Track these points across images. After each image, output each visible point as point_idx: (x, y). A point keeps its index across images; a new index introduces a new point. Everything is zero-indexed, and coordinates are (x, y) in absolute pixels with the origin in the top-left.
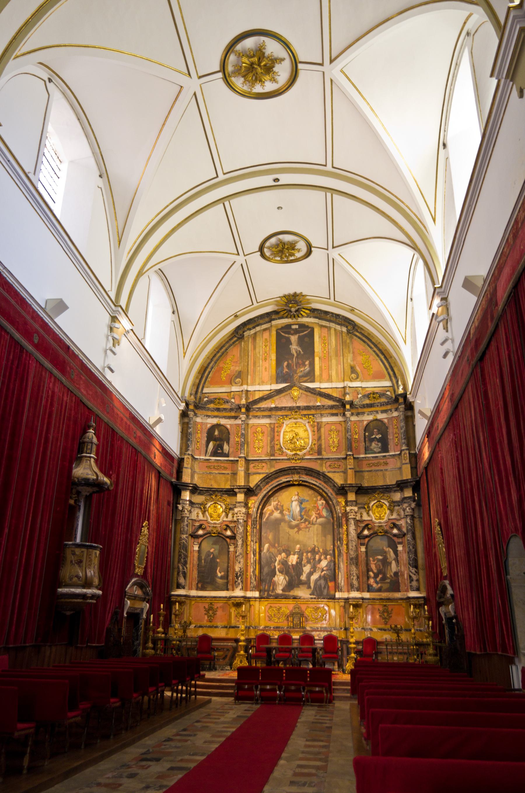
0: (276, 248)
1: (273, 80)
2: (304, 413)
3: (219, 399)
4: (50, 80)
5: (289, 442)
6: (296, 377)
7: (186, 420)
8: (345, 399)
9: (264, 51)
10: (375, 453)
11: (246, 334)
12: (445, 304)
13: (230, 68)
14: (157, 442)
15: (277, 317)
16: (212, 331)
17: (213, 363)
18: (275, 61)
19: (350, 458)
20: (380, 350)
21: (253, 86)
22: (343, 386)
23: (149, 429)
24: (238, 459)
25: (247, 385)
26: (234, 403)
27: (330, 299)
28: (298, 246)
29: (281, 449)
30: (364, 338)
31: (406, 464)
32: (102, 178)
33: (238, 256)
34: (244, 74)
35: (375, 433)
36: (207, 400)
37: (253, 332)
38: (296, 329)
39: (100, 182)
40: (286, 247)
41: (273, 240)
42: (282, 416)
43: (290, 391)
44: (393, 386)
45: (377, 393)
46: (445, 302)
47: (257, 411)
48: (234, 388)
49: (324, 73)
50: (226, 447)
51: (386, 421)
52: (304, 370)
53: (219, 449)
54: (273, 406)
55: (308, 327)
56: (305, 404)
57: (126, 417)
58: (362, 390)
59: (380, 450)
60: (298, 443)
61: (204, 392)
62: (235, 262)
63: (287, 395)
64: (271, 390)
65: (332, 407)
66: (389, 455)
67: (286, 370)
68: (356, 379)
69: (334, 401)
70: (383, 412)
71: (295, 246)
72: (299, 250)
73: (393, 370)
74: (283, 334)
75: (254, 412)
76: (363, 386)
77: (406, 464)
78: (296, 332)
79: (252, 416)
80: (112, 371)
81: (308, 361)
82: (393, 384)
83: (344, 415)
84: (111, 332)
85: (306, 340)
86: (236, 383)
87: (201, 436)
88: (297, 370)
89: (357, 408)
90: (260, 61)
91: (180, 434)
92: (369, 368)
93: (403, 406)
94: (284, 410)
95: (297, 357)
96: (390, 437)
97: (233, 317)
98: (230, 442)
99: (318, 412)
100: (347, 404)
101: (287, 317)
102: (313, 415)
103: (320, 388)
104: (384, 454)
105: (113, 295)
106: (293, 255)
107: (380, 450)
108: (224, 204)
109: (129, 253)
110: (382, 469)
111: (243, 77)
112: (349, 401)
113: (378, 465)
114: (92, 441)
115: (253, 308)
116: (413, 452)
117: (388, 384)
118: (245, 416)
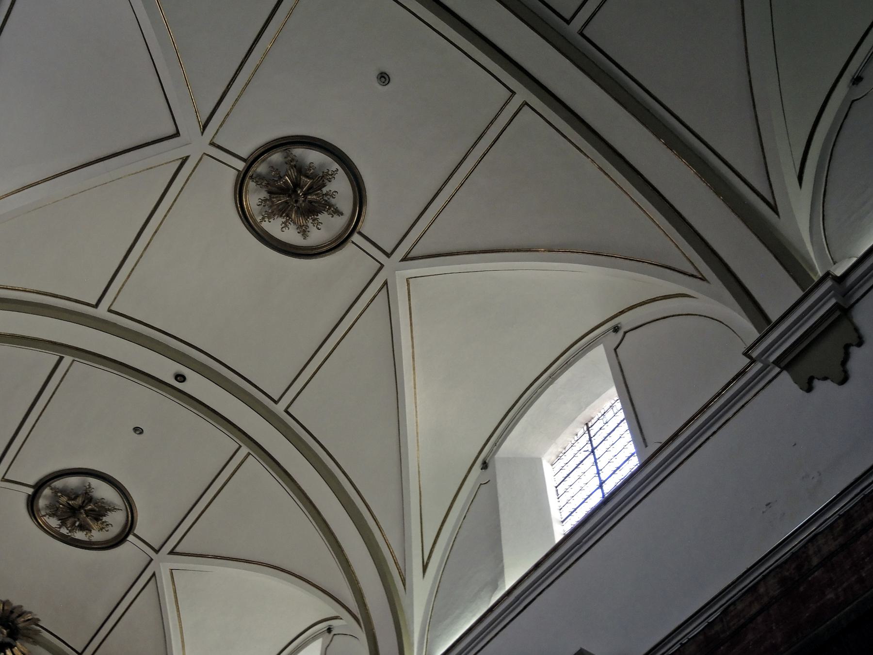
1: (304, 231)
13: (261, 168)
21: (270, 216)
28: (110, 518)
34: (274, 189)
41: (73, 482)
108: (61, 358)
111: (269, 192)
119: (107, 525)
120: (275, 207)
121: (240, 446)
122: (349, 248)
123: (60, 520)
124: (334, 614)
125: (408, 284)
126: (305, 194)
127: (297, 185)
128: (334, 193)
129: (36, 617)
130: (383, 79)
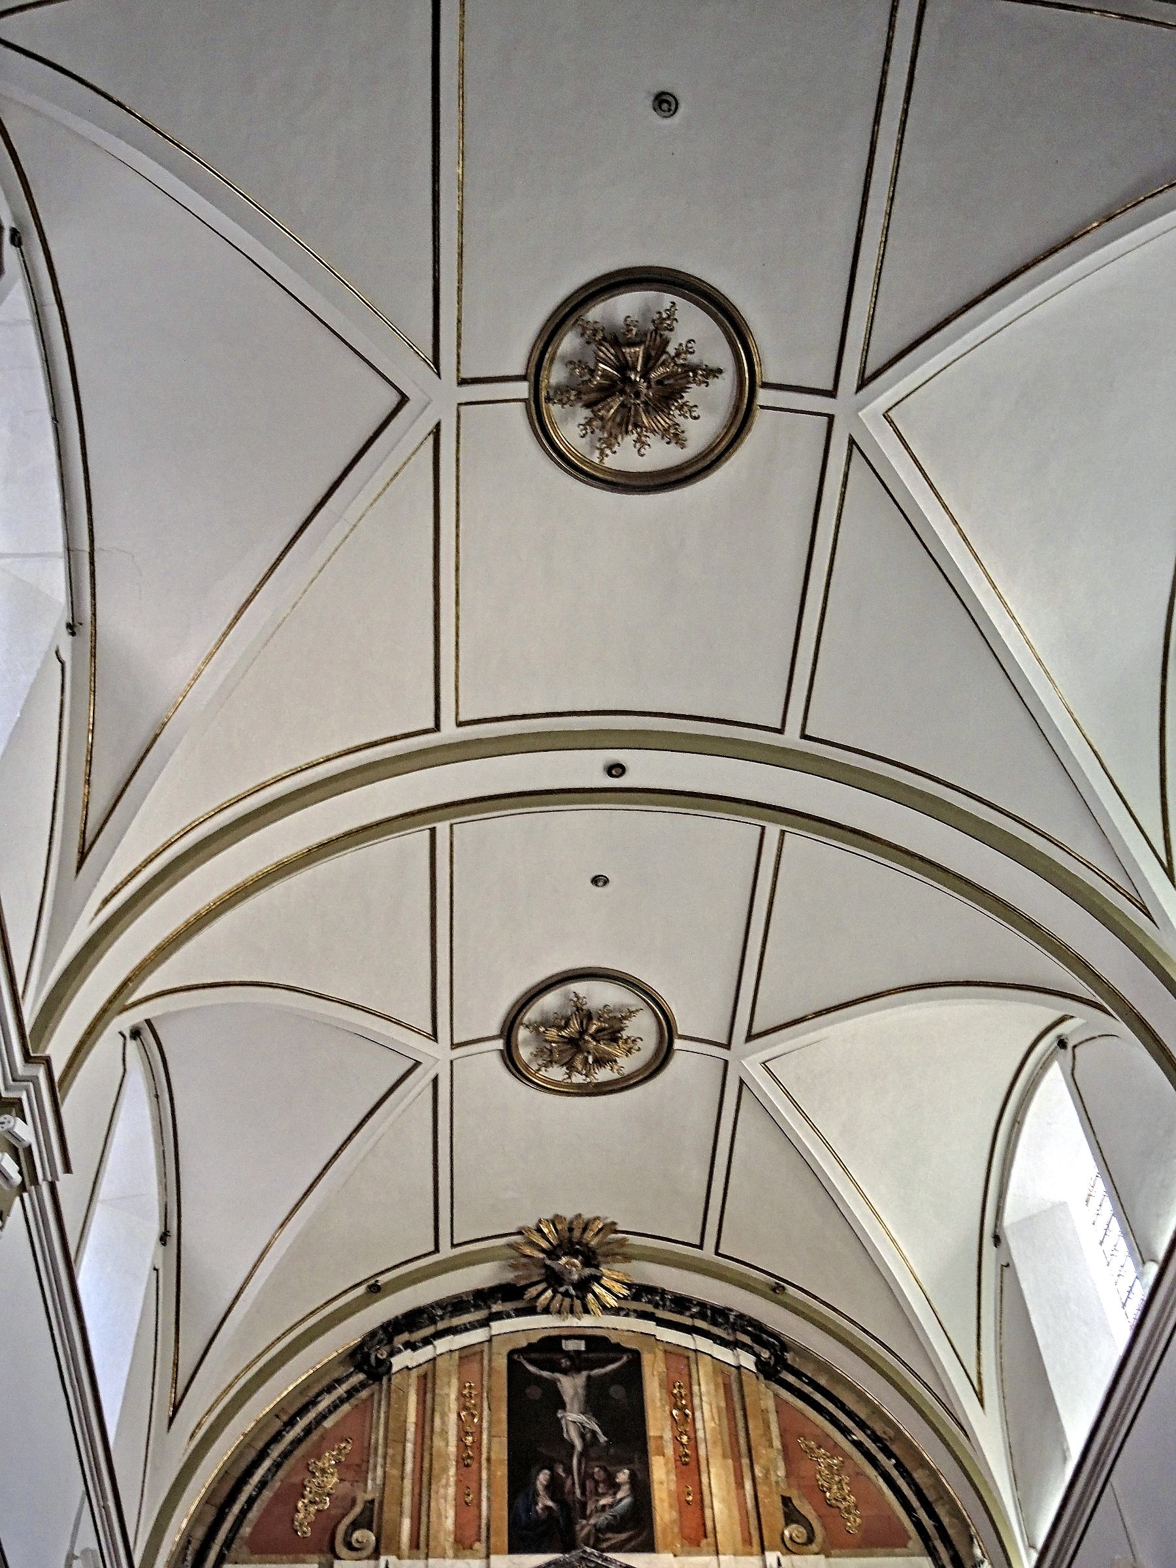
11: (398, 1362)
13: (556, 375)
15: (509, 1306)
16: (284, 1334)
17: (267, 1464)
21: (609, 443)
25: (399, 1557)
27: (701, 1247)
28: (631, 1029)
30: (818, 1397)
32: (73, 634)
34: (593, 396)
37: (426, 1353)
38: (578, 1352)
39: (65, 642)
40: (593, 1028)
41: (551, 1001)
52: (611, 1506)
55: (619, 1349)
67: (545, 1502)
68: (803, 1544)
71: (622, 1029)
73: (933, 1515)
78: (577, 1363)
86: (349, 1546)
88: (584, 1505)
90: (650, 364)
92: (845, 1504)
95: (581, 1454)
97: (361, 1290)
101: (546, 1311)
108: (433, 831)
109: (106, 901)
111: (588, 405)
115: (437, 1263)
119: (634, 1040)
120: (610, 424)
121: (763, 828)
122: (761, 420)
123: (562, 1066)
124: (1058, 1014)
125: (891, 422)
127: (624, 367)
128: (689, 345)
129: (609, 1221)
130: (665, 106)
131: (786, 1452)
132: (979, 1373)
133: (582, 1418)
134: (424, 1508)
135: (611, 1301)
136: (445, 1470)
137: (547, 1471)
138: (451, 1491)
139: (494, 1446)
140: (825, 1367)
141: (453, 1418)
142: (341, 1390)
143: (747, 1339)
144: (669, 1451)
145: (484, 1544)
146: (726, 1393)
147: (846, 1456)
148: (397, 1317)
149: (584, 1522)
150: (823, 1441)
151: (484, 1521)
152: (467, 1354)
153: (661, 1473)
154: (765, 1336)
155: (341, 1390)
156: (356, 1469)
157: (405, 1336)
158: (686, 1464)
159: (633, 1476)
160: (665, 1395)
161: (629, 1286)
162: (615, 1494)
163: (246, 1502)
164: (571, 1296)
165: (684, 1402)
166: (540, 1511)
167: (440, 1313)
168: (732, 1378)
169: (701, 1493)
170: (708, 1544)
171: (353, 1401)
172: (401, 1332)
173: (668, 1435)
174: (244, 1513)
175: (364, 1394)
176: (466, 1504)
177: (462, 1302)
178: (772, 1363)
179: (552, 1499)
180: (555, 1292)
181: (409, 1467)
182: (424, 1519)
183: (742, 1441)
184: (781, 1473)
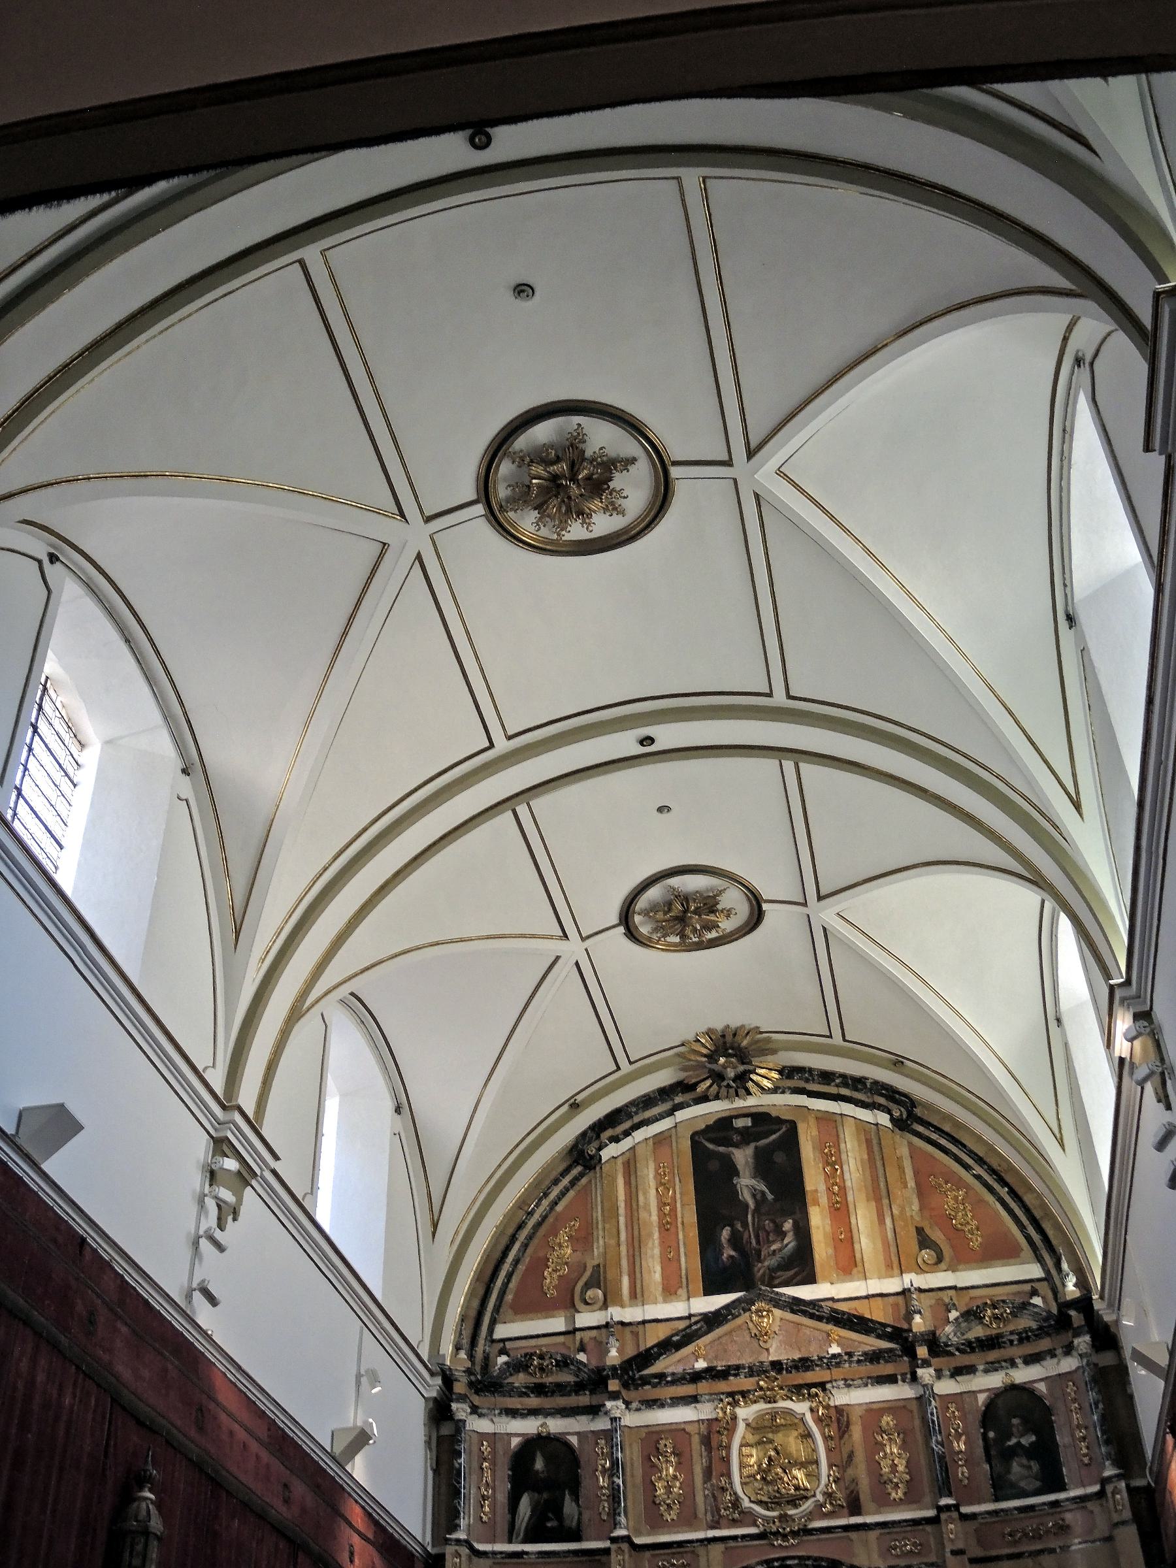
0: (665, 913)
1: (613, 508)
2: (796, 1383)
3: (541, 1357)
4: (53, 558)
5: (758, 1477)
6: (761, 1272)
7: (447, 1429)
8: (910, 1330)
9: (581, 446)
10: (1025, 1494)
11: (606, 1154)
12: (1148, 1030)
13: (502, 492)
14: (358, 1510)
15: (688, 1097)
17: (517, 1246)
18: (611, 465)
19: (950, 1517)
20: (992, 1171)
21: (563, 526)
22: (899, 1289)
23: (332, 1468)
24: (606, 1544)
25: (622, 1306)
26: (585, 1365)
28: (725, 902)
29: (736, 1503)
30: (943, 1142)
31: (1123, 1523)
32: (189, 775)
33: (565, 942)
34: (538, 501)
35: (1014, 1430)
36: (506, 1363)
38: (746, 1128)
41: (654, 893)
42: (731, 1394)
43: (747, 1314)
44: (1048, 1278)
45: (1004, 1301)
46: (1146, 1024)
47: (654, 1386)
48: (587, 1318)
49: (735, 481)
50: (569, 1507)
51: (1042, 1387)
52: (780, 1250)
53: (550, 1515)
54: (701, 1364)
55: (779, 1121)
56: (797, 1356)
57: (258, 1440)
58: (958, 1295)
59: (1038, 1484)
60: (786, 1479)
61: (496, 1336)
62: (558, 958)
63: (739, 1327)
64: (690, 1316)
65: (874, 1357)
66: (1067, 1499)
67: (728, 1252)
69: (879, 1337)
70: (1032, 1359)
72: (728, 913)
74: (711, 1146)
75: (647, 1387)
76: (959, 1285)
77: (1123, 1523)
78: (746, 1136)
79: (642, 1402)
80: (213, 1300)
81: (791, 1221)
82: (1047, 1272)
83: (914, 1378)
84: (211, 1185)
85: (779, 1157)
86: (587, 1303)
87: (494, 1481)
88: (760, 1251)
89: (952, 1354)
90: (576, 469)
91: (430, 1474)
93: (1087, 1338)
94: (736, 1375)
95: (757, 1210)
96: (1062, 1439)
97: (566, 1107)
98: (583, 1491)
99: (836, 1373)
100: (921, 1345)
102: (822, 1385)
103: (832, 1299)
104: (1052, 1497)
105: (217, 1080)
106: (710, 926)
107: (1038, 1484)
110: (1052, 1546)
111: (535, 509)
112: (922, 1334)
113: (1038, 1537)
114: (147, 1527)
116: (1138, 1483)
117: (1035, 1272)
118: (620, 1403)
126: (573, 478)
129: (752, 1026)
131: (921, 1192)
132: (1059, 1126)
133: (753, 1182)
134: (638, 1264)
135: (767, 1084)
136: (650, 1235)
137: (728, 1228)
138: (657, 1251)
139: (688, 1215)
140: (949, 1118)
141: (653, 1192)
142: (565, 1181)
143: (882, 1101)
144: (824, 1200)
145: (685, 1290)
146: (868, 1148)
147: (968, 1187)
148: (600, 1119)
149: (760, 1265)
150: (950, 1177)
151: (684, 1272)
152: (660, 1140)
153: (819, 1220)
154: (897, 1096)
155: (565, 1181)
156: (584, 1240)
157: (609, 1133)
158: (838, 1209)
159: (796, 1226)
160: (817, 1154)
161: (780, 1072)
162: (783, 1240)
163: (506, 1276)
164: (732, 1087)
165: (833, 1159)
166: (725, 1259)
167: (634, 1109)
168: (873, 1133)
169: (851, 1231)
170: (859, 1272)
171: (577, 1188)
172: (605, 1129)
173: (822, 1187)
174: (506, 1285)
175: (584, 1181)
176: (669, 1261)
177: (650, 1098)
178: (904, 1116)
179: (735, 1250)
180: (720, 1087)
181: (623, 1236)
182: (638, 1275)
183: (882, 1185)
184: (916, 1207)
